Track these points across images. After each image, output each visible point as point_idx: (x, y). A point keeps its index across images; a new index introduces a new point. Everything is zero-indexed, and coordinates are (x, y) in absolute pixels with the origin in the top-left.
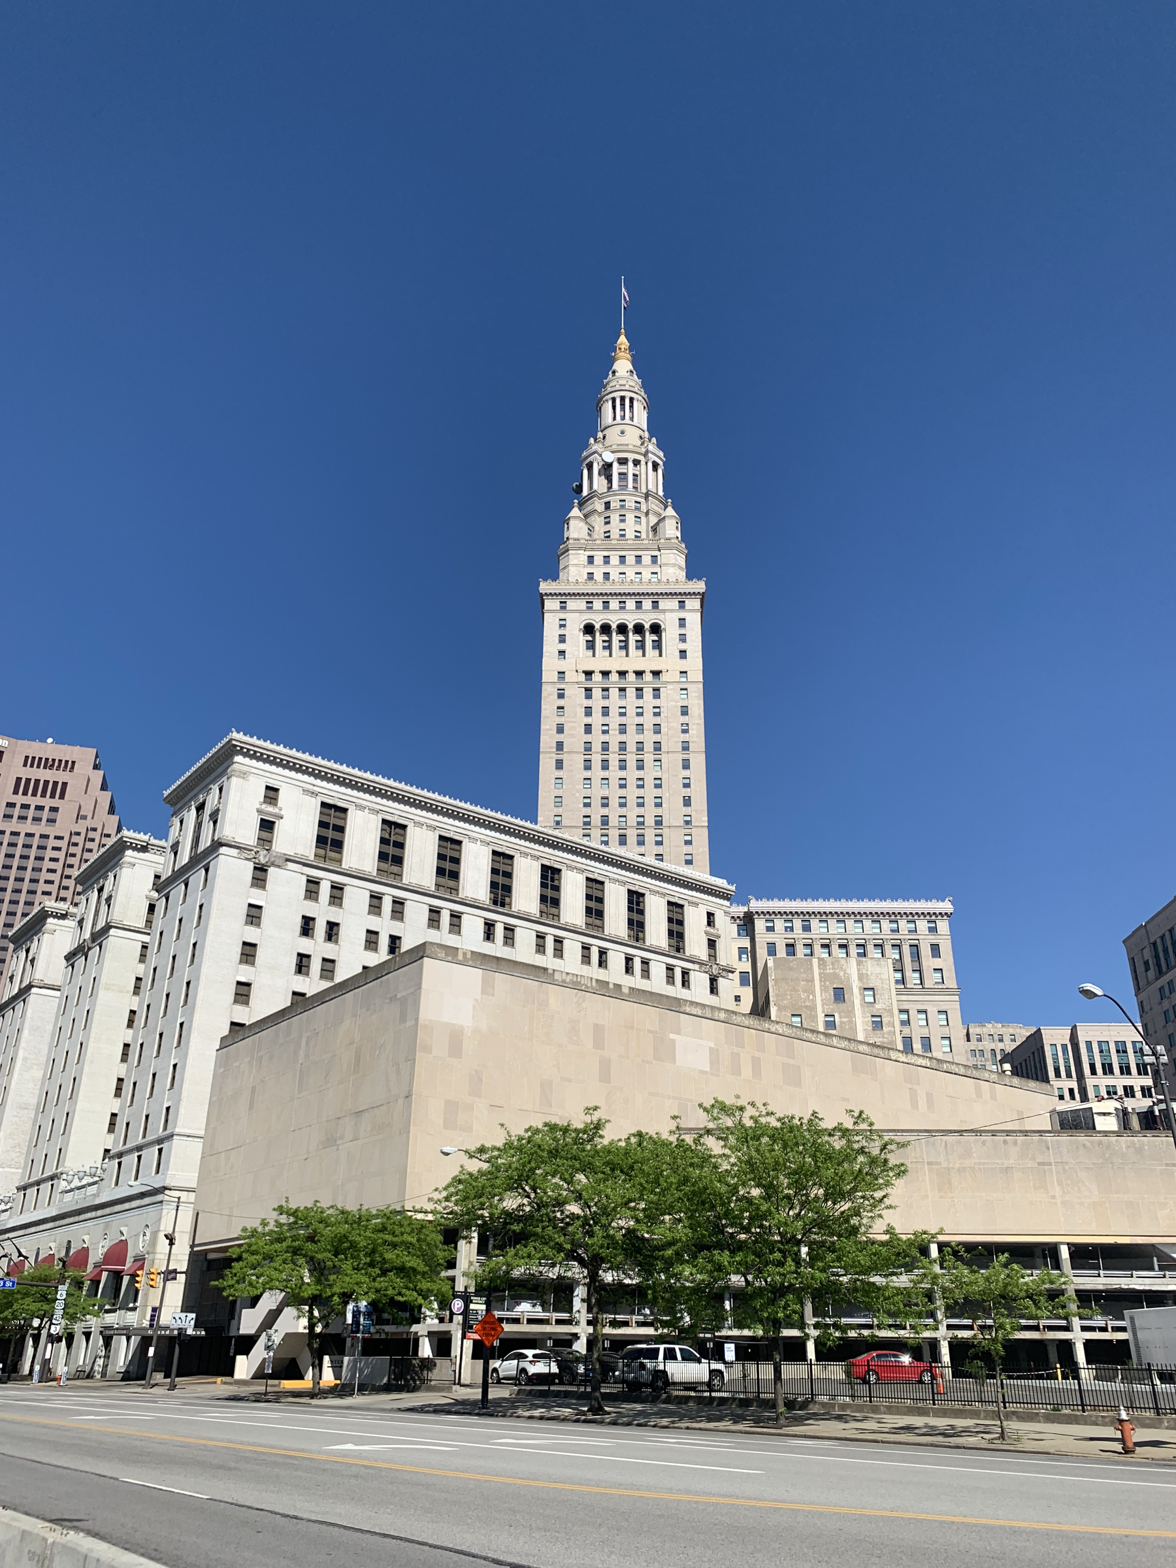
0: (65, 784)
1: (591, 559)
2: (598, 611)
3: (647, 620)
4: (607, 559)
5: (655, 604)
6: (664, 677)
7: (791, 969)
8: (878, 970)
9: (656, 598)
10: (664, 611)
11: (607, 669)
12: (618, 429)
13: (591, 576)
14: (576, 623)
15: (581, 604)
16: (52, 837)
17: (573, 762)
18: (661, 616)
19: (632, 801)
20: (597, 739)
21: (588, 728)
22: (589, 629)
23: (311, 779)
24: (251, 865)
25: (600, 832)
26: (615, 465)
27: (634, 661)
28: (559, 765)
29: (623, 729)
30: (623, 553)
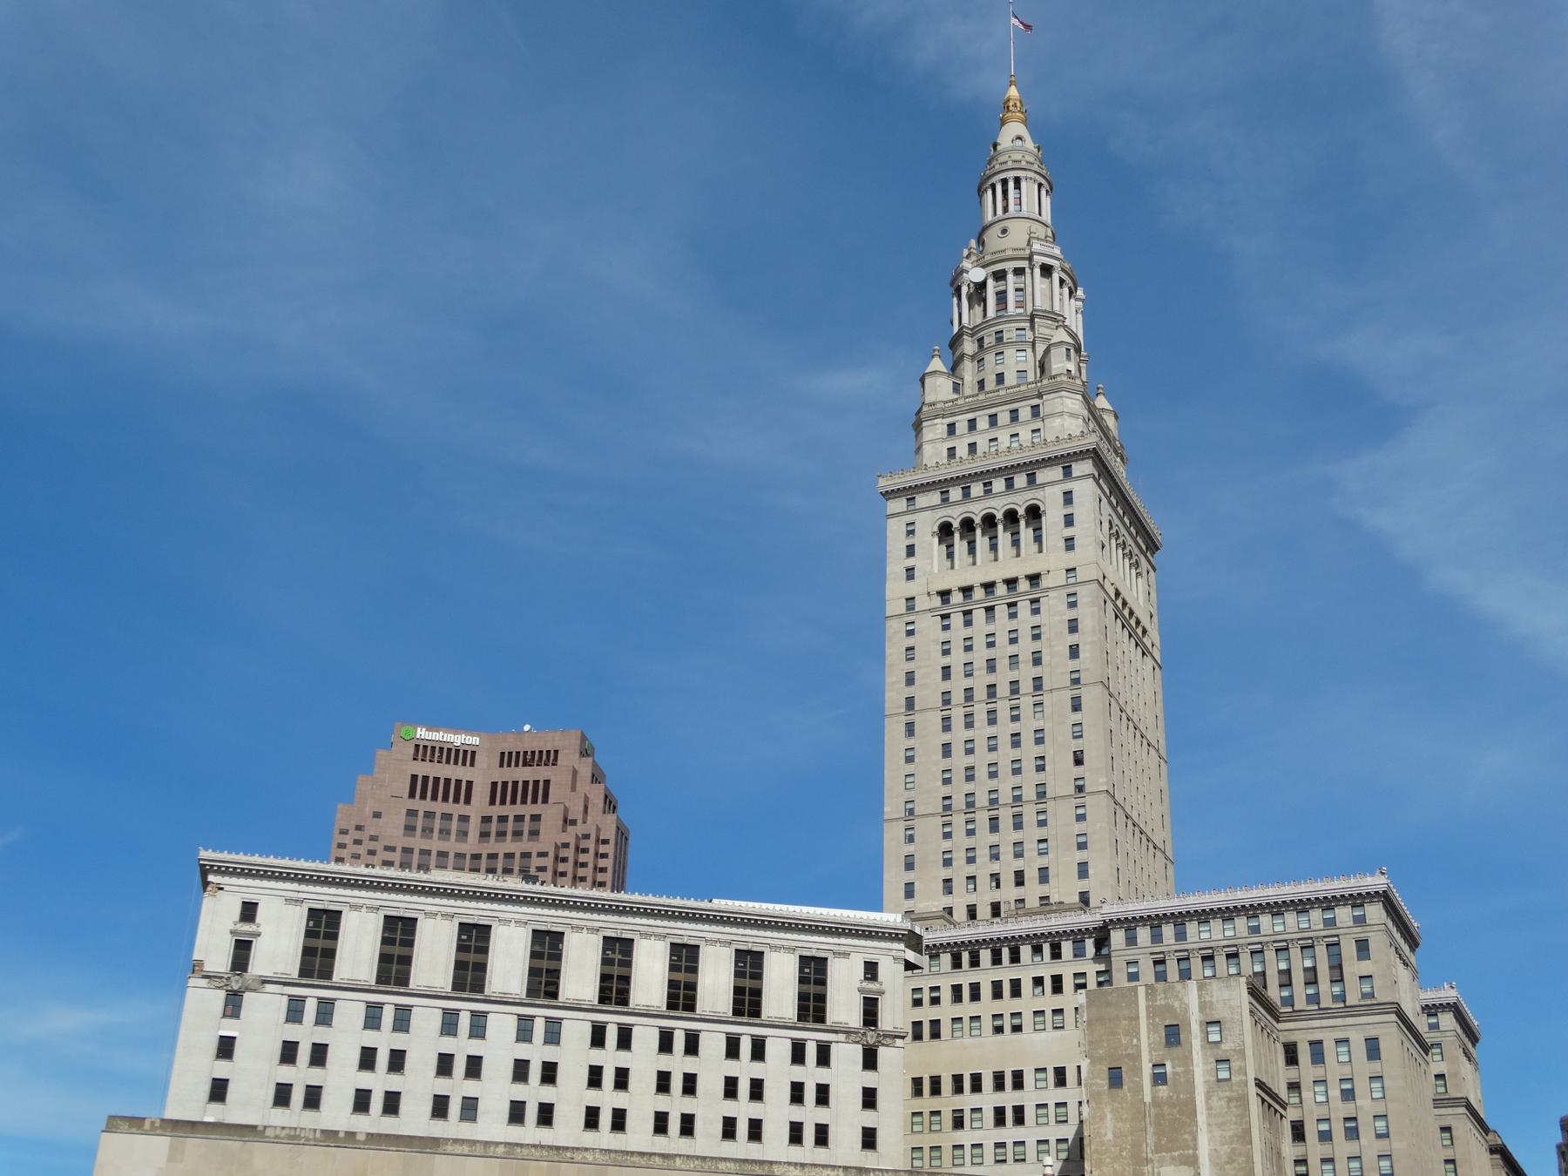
0: (547, 782)
1: (951, 428)
2: (956, 503)
4: (972, 424)
5: (1031, 478)
6: (1045, 582)
7: (1109, 1004)
8: (1226, 995)
9: (1030, 469)
10: (1043, 485)
13: (952, 452)
14: (927, 524)
15: (934, 498)
16: (534, 855)
17: (928, 723)
18: (1039, 494)
19: (1005, 768)
20: (958, 684)
21: (946, 672)
22: (945, 531)
23: (295, 886)
24: (222, 994)
25: (963, 818)
26: (990, 282)
27: (1008, 564)
28: (910, 729)
29: (991, 665)
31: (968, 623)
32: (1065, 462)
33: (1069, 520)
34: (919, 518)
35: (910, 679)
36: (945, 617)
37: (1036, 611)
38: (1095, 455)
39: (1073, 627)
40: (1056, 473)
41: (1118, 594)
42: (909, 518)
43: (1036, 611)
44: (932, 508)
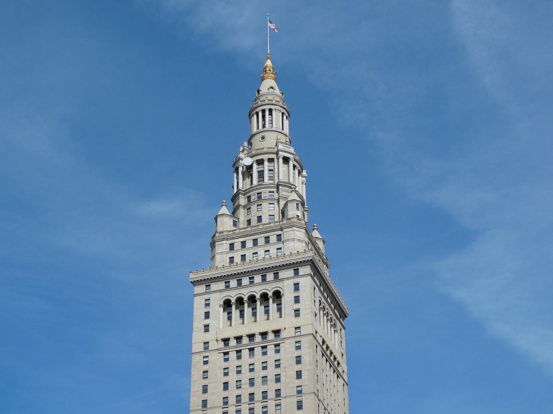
1: (232, 246)
3: (269, 289)
4: (243, 244)
5: (276, 275)
6: (283, 335)
9: (276, 270)
11: (251, 332)
12: (259, 137)
13: (232, 259)
14: (217, 300)
15: (221, 285)
18: (280, 284)
20: (232, 393)
21: (226, 386)
22: (227, 304)
26: (255, 166)
27: (263, 324)
29: (252, 382)
30: (255, 237)
31: (239, 357)
32: (295, 266)
33: (297, 300)
34: (212, 296)
35: (205, 390)
36: (226, 354)
37: (278, 351)
38: (312, 263)
39: (299, 360)
40: (290, 273)
41: (324, 342)
42: (207, 297)
43: (278, 351)
44: (220, 291)
